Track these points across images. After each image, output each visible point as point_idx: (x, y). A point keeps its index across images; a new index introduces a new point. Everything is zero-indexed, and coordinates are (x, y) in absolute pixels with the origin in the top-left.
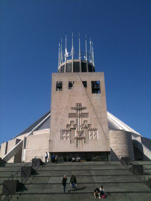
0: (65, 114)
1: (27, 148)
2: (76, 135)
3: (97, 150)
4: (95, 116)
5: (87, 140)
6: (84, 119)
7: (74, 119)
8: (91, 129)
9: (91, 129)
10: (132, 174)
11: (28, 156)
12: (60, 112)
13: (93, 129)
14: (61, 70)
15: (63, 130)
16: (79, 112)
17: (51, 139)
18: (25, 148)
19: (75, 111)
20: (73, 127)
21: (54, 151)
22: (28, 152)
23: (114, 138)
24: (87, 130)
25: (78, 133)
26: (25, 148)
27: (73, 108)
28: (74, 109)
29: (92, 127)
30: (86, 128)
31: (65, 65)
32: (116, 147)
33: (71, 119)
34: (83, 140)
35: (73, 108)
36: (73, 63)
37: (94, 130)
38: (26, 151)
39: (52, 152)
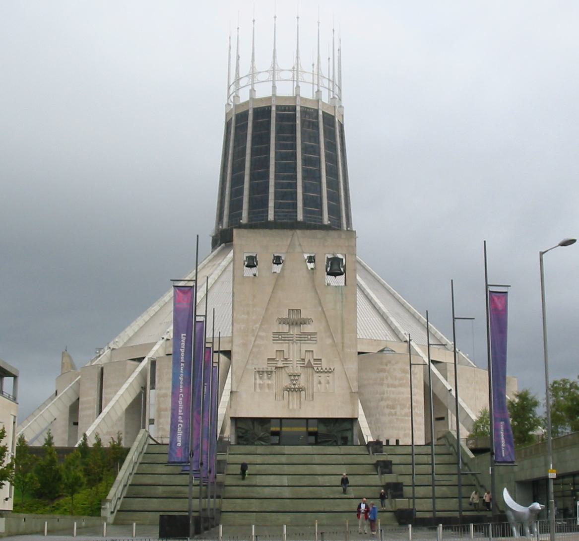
0: (262, 334)
1: (160, 389)
2: (286, 382)
3: (330, 417)
4: (329, 341)
5: (310, 392)
6: (305, 347)
7: (284, 347)
8: (320, 368)
9: (320, 368)
10: (374, 473)
11: (163, 406)
12: (253, 330)
13: (324, 369)
14: (236, 128)
15: (259, 372)
16: (295, 331)
17: (234, 390)
18: (153, 388)
19: (285, 328)
20: (282, 366)
21: (240, 416)
22: (162, 399)
23: (378, 372)
24: (310, 370)
25: (292, 378)
26: (153, 388)
27: (282, 321)
28: (284, 323)
29: (324, 365)
30: (310, 366)
31: (251, 112)
32: (380, 395)
33: (277, 347)
34: (303, 393)
35: (282, 321)
36: (274, 109)
37: (326, 372)
38: (159, 396)
39: (237, 416)
